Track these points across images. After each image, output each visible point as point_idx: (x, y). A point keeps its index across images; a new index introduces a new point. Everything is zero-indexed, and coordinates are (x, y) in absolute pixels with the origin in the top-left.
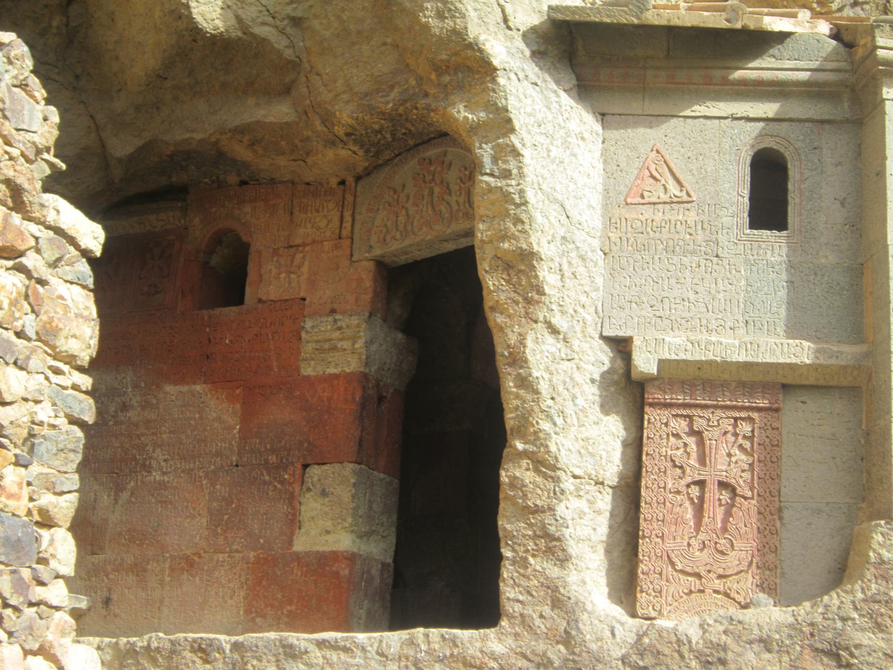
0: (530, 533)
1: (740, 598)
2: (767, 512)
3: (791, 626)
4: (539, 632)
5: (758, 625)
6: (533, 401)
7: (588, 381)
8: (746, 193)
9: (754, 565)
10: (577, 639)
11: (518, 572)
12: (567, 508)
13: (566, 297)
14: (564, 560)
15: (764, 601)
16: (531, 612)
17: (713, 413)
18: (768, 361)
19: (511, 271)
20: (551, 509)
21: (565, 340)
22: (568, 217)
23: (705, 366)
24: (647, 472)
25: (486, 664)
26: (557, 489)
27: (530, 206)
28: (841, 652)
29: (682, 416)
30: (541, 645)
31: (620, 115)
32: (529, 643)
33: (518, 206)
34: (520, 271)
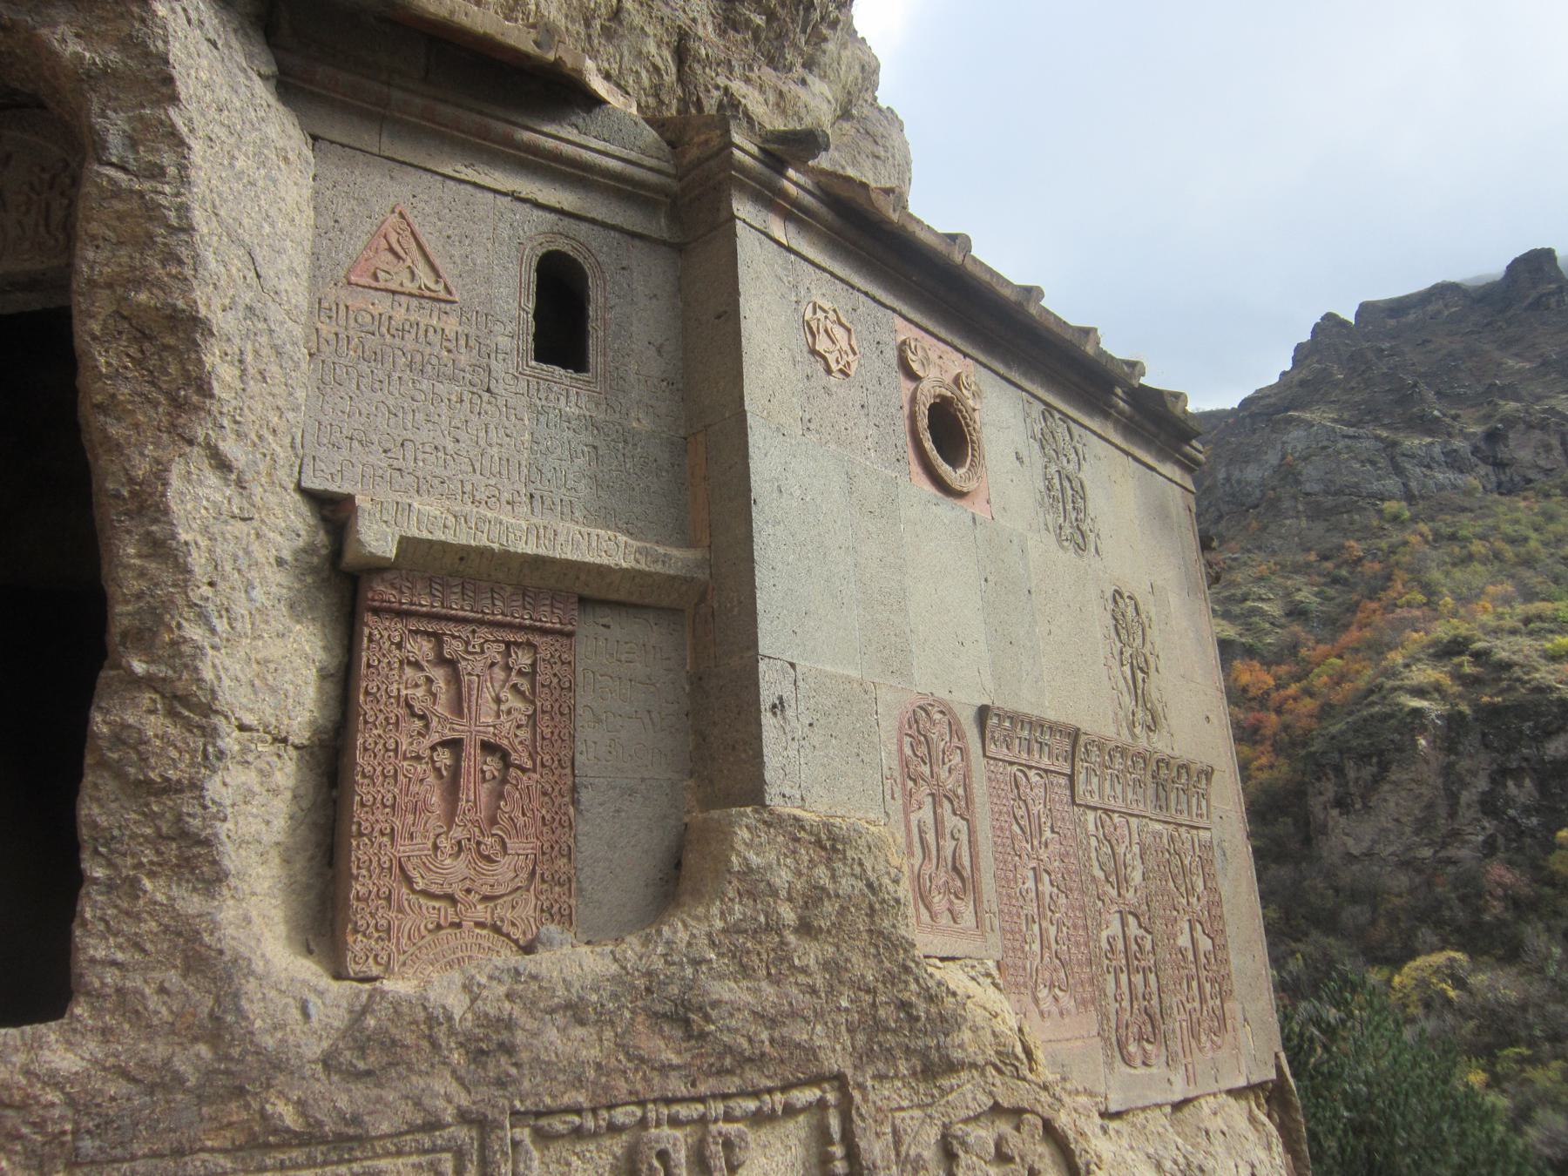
0: (148, 831)
1: (517, 934)
2: (556, 793)
4: (155, 1021)
5: (564, 980)
6: (174, 585)
7: (272, 560)
11: (116, 906)
12: (225, 784)
13: (246, 411)
14: (212, 879)
15: (558, 937)
16: (139, 983)
17: (474, 632)
18: (569, 557)
19: (147, 345)
20: (196, 786)
21: (240, 484)
22: (258, 276)
24: (366, 722)
25: (35, 1097)
26: (210, 749)
28: (692, 1016)
29: (426, 633)
30: (160, 1048)
32: (131, 1046)
33: (173, 230)
34: (166, 347)
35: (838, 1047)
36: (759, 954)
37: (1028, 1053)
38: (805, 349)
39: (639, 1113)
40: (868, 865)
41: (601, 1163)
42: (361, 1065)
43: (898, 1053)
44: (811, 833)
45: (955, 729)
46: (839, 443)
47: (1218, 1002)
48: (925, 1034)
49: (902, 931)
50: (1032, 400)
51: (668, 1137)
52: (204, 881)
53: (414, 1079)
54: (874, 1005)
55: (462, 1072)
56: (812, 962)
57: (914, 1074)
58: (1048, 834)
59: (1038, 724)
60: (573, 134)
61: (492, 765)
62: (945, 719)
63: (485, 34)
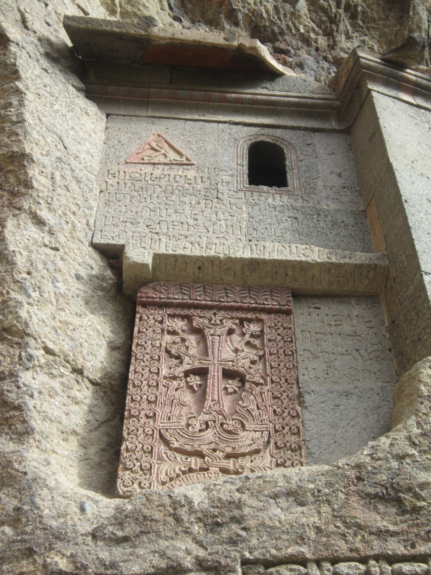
6: (5, 272)
7: (73, 275)
8: (246, 163)
9: (272, 444)
10: (30, 514)
12: (34, 378)
13: (55, 199)
14: (24, 433)
17: (215, 314)
18: (276, 258)
20: (13, 375)
22: (66, 148)
23: (206, 264)
26: (23, 354)
27: (26, 124)
29: (179, 316)
31: (124, 116)
33: (14, 123)
39: (362, 567)
42: (120, 534)
52: (18, 433)
53: (161, 542)
55: (201, 538)
60: (265, 91)
61: (233, 385)
63: (194, 41)
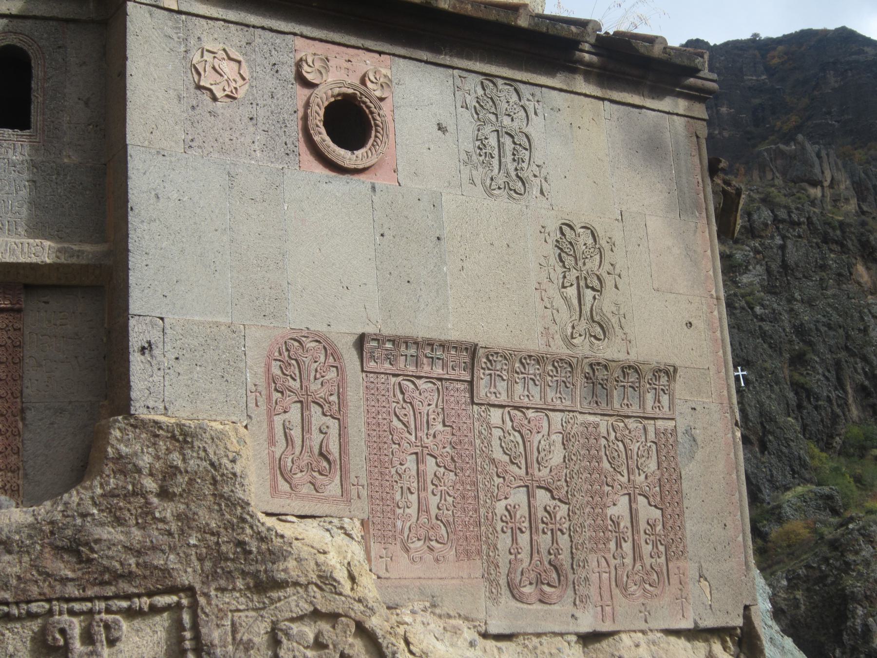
2: (9, 414)
3: (30, 526)
15: (6, 503)
28: (81, 548)
35: (189, 570)
36: (129, 510)
37: (352, 578)
38: (193, 86)
39: (47, 606)
40: (211, 451)
41: (24, 635)
43: (236, 574)
44: (168, 431)
45: (330, 350)
46: (222, 151)
47: (663, 560)
48: (257, 562)
49: (240, 494)
50: (464, 74)
51: (66, 621)
54: (217, 543)
56: (168, 515)
57: (248, 588)
58: (440, 427)
59: (443, 345)
62: (321, 346)
